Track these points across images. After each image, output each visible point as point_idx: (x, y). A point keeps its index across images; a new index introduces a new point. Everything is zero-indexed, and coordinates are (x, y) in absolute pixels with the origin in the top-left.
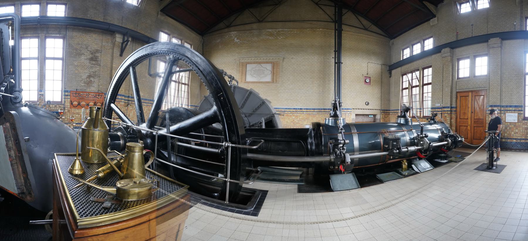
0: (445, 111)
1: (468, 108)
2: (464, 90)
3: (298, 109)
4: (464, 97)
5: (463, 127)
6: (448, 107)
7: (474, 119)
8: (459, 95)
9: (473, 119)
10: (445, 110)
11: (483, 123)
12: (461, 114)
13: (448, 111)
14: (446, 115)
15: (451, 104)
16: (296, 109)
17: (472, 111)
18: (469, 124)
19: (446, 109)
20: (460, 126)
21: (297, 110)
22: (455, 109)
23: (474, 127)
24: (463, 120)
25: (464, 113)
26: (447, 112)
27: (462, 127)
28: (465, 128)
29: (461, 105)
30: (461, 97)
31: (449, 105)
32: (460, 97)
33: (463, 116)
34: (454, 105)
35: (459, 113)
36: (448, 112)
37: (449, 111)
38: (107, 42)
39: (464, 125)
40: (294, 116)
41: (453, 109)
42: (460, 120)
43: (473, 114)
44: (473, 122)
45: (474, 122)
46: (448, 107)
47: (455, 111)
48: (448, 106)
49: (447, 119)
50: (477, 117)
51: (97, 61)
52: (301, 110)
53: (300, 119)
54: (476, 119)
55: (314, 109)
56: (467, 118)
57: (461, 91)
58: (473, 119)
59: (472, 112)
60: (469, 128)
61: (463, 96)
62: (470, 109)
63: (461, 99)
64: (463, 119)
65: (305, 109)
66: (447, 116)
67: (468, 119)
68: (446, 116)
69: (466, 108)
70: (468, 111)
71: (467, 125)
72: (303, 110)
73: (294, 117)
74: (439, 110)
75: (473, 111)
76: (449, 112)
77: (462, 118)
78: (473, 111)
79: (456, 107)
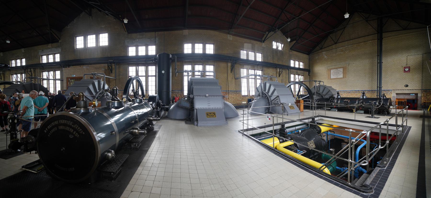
3: (357, 91)
16: (356, 91)
21: (356, 91)
38: (274, 72)
40: (355, 94)
51: (272, 80)
52: (359, 91)
53: (358, 96)
55: (366, 91)
65: (361, 91)
72: (360, 91)
73: (355, 95)
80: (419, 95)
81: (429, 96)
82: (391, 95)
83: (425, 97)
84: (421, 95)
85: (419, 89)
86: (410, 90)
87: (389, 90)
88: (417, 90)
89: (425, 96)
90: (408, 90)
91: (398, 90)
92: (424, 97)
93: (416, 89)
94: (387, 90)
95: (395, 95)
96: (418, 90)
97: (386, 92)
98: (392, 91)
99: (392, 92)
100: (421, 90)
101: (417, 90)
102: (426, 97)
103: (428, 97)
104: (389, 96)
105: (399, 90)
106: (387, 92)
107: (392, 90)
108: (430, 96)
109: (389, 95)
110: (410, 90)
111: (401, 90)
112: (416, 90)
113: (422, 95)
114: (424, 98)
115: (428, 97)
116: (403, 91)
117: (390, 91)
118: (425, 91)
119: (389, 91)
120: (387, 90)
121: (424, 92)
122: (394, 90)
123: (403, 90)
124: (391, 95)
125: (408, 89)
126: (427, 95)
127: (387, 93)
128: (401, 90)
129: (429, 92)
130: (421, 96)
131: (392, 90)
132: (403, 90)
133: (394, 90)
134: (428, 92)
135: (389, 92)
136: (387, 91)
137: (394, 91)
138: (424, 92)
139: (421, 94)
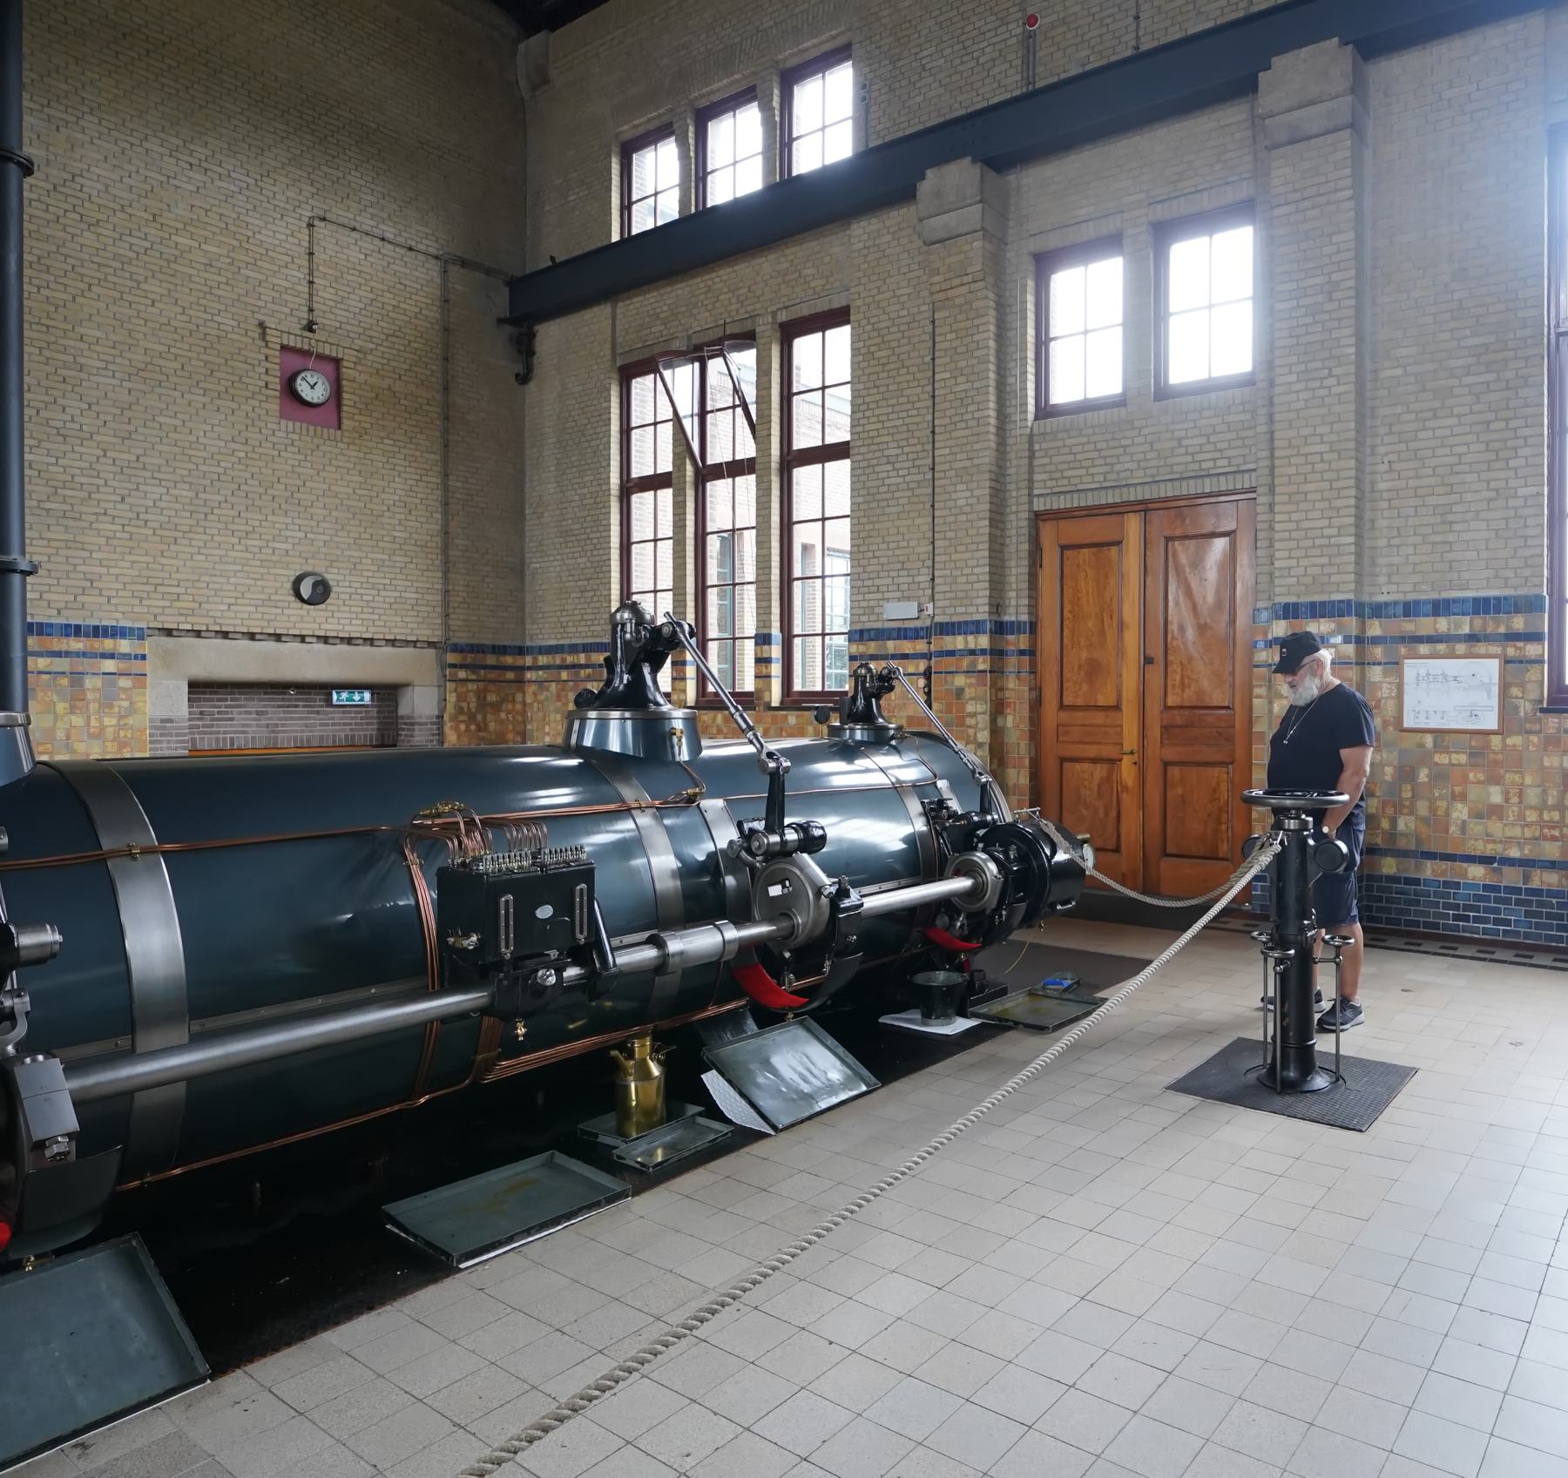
0: (951, 653)
1: (1121, 627)
2: (1091, 500)
4: (1085, 551)
5: (1086, 766)
6: (975, 628)
7: (1167, 708)
8: (1048, 533)
9: (1154, 709)
10: (950, 648)
11: (1230, 739)
12: (1067, 674)
13: (972, 652)
14: (960, 681)
15: (997, 606)
17: (1151, 653)
18: (1127, 748)
19: (959, 642)
20: (1063, 760)
22: (1023, 641)
23: (1167, 764)
24: (1080, 714)
25: (1094, 670)
26: (965, 662)
27: (1078, 766)
28: (1100, 771)
29: (1067, 607)
30: (1068, 553)
31: (980, 610)
32: (1057, 551)
33: (1085, 687)
34: (1017, 610)
35: (1056, 669)
36: (974, 663)
37: (983, 652)
39: (1091, 751)
41: (1011, 638)
42: (1064, 716)
43: (1155, 675)
44: (1155, 732)
45: (1166, 728)
46: (975, 628)
47: (1022, 653)
48: (976, 617)
49: (970, 708)
50: (1189, 696)
54: (1182, 707)
56: (1112, 701)
57: (1062, 503)
58: (1154, 709)
59: (1148, 660)
60: (1127, 772)
61: (1080, 546)
62: (1132, 639)
63: (1067, 563)
64: (1088, 708)
66: (969, 692)
67: (1117, 708)
68: (960, 692)
69: (1102, 633)
70: (1120, 652)
71: (1108, 751)
74: (907, 647)
75: (1157, 652)
76: (981, 659)
77: (1080, 702)
78: (1157, 652)
79: (1033, 627)
80: (421, 703)
81: (497, 707)
82: (132, 710)
83: (473, 727)
84: (443, 700)
85: (424, 634)
86: (349, 641)
87: (97, 632)
88: (407, 643)
89: (472, 717)
90: (325, 640)
91: (220, 642)
92: (463, 727)
93: (400, 633)
94: (77, 631)
95: (178, 704)
96: (410, 650)
97: (63, 664)
98: (147, 647)
99: (147, 667)
100: (432, 651)
101: (407, 643)
102: (479, 729)
103: (489, 717)
104: (107, 721)
105: (225, 635)
106: (84, 664)
107: (140, 635)
108: (503, 715)
109: (106, 704)
110: (349, 641)
111: (252, 636)
112: (392, 642)
113: (452, 698)
114: (468, 729)
115: (492, 726)
116: (271, 645)
117: (124, 646)
118: (470, 658)
119: (108, 644)
120: (77, 631)
121: (462, 674)
122: (169, 632)
123: (278, 637)
124: (132, 710)
125: (330, 628)
126: (482, 704)
127: (77, 677)
128: (252, 636)
129: (494, 667)
130: (441, 717)
131: (140, 635)
132: (278, 637)
133: (169, 632)
134: (493, 675)
135: (109, 665)
136: (76, 645)
137: (164, 640)
138: (462, 666)
139: (441, 687)
